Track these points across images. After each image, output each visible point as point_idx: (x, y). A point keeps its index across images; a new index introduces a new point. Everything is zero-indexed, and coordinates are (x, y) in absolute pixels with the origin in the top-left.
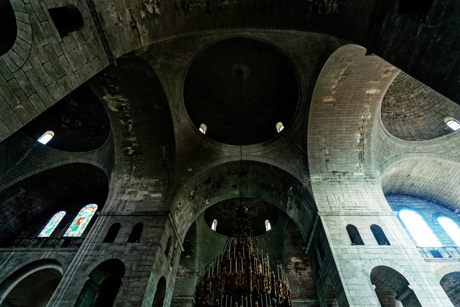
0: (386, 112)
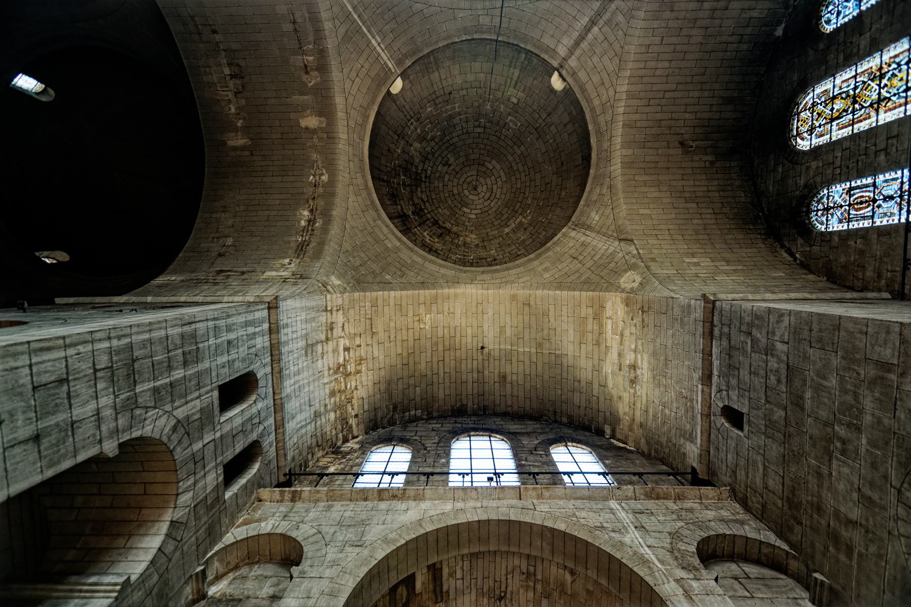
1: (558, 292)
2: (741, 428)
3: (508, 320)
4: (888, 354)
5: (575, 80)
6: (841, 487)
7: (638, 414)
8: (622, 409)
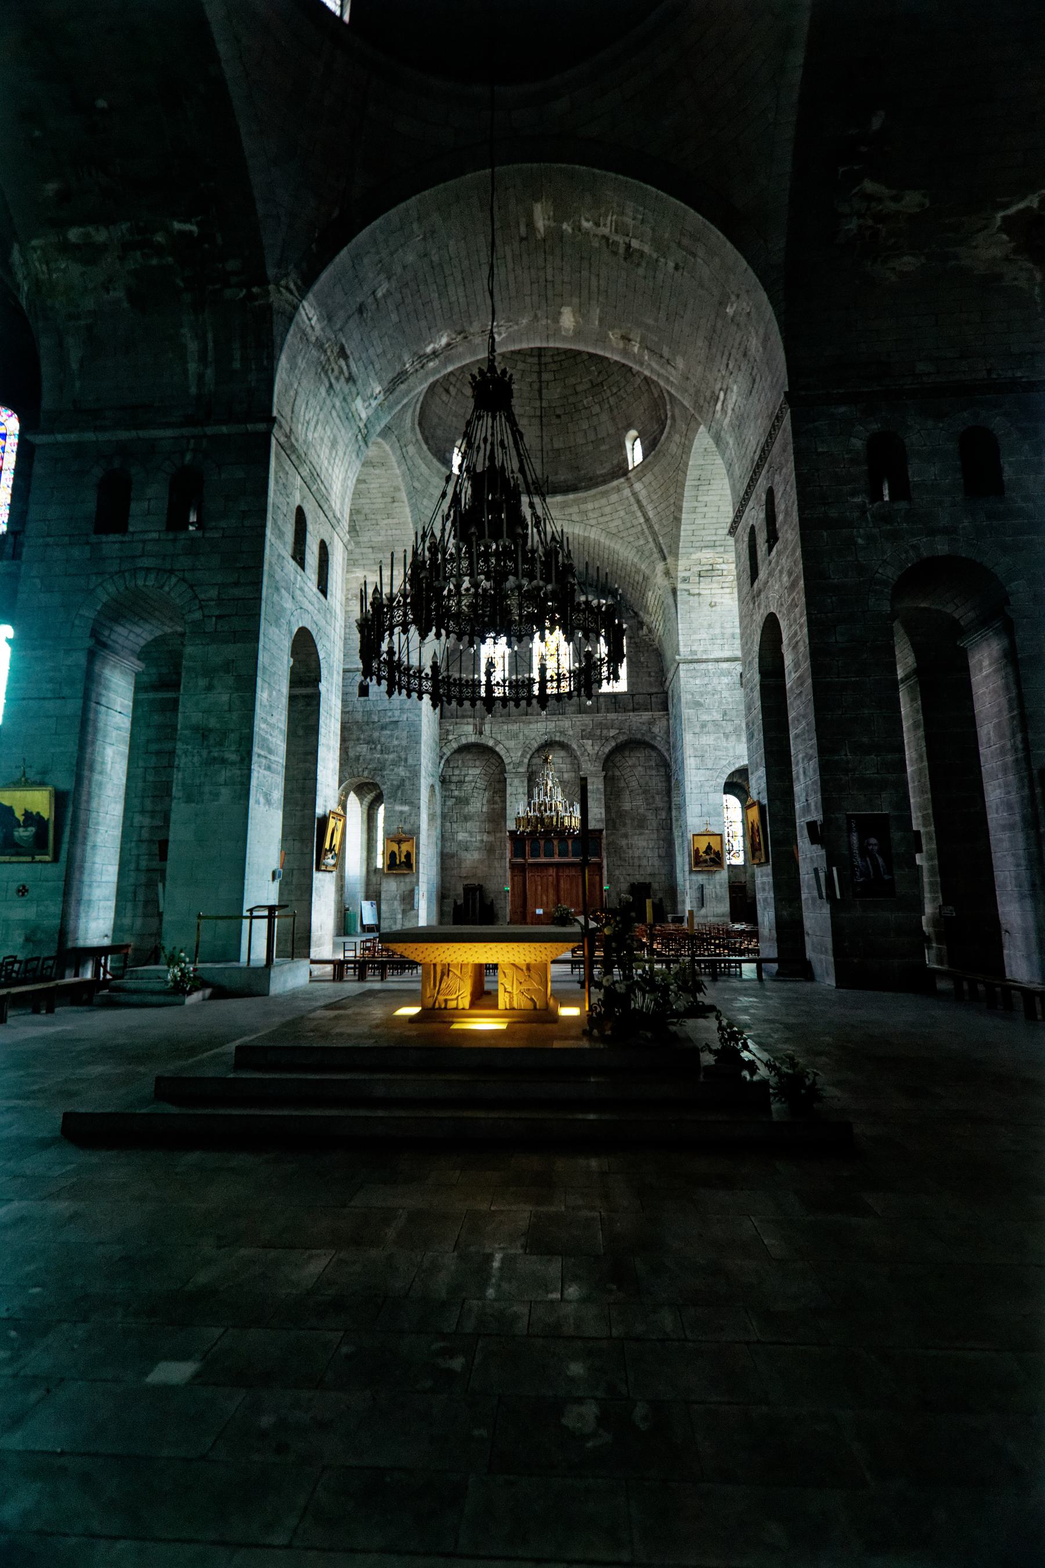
3: (372, 486)
4: (410, 761)
5: (613, 488)
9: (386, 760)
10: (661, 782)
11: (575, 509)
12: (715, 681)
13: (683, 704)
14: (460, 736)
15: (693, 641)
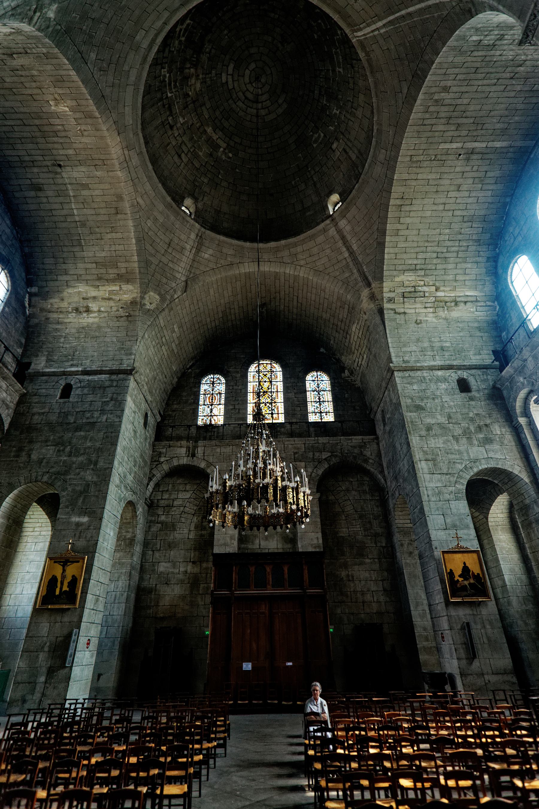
0: (170, 76)
1: (134, 241)
2: (61, 398)
3: (97, 192)
4: (101, 464)
5: (320, 231)
6: (44, 451)
7: (55, 316)
8: (54, 302)
9: (74, 463)
10: (377, 506)
11: (286, 253)
12: (433, 386)
13: (404, 409)
14: (172, 458)
15: (404, 352)
